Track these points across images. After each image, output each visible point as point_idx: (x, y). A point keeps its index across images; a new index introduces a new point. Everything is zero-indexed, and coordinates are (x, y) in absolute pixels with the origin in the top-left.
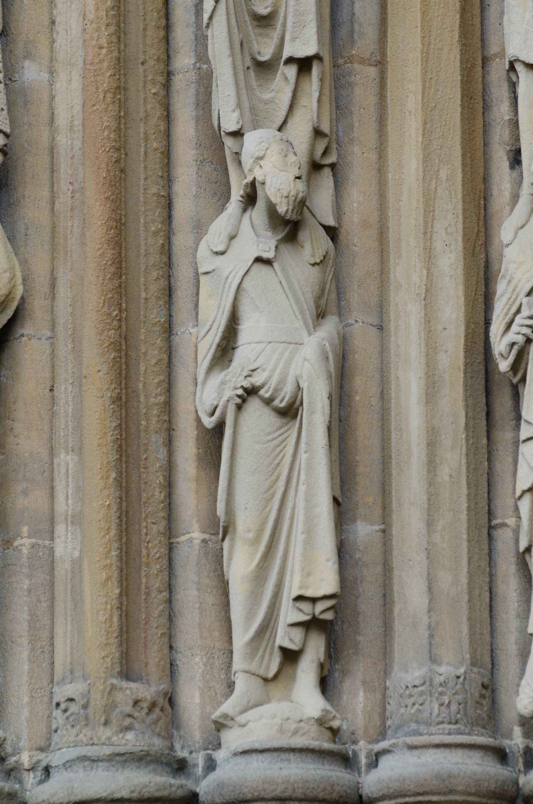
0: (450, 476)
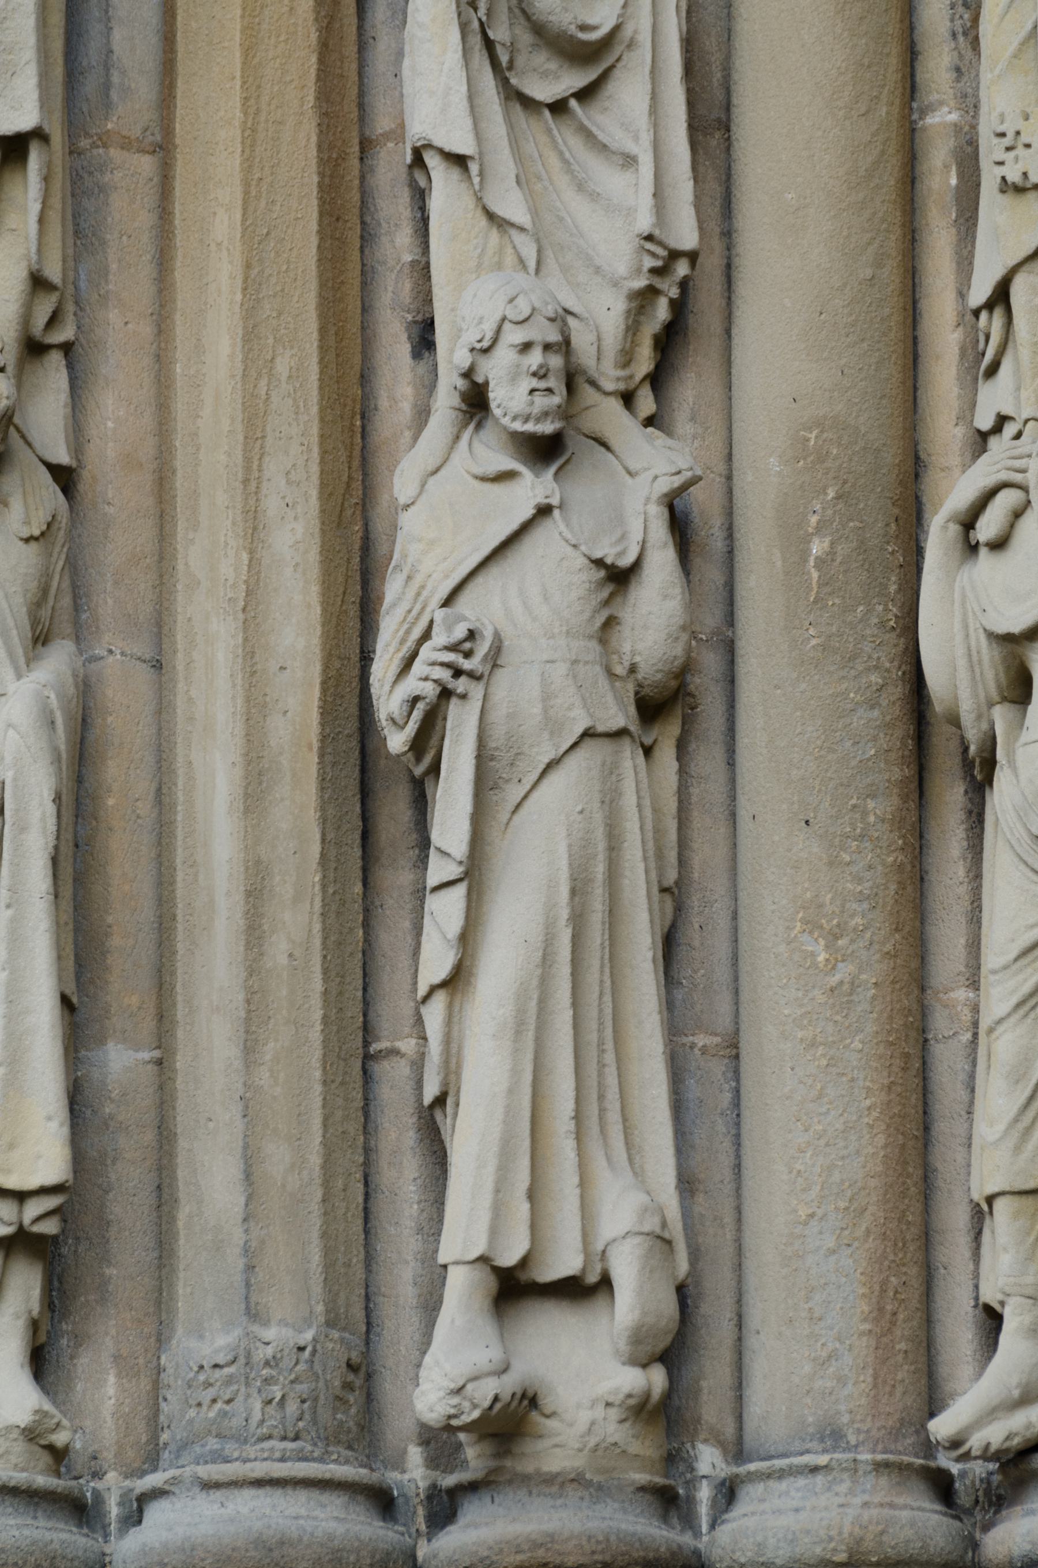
0: (290, 955)
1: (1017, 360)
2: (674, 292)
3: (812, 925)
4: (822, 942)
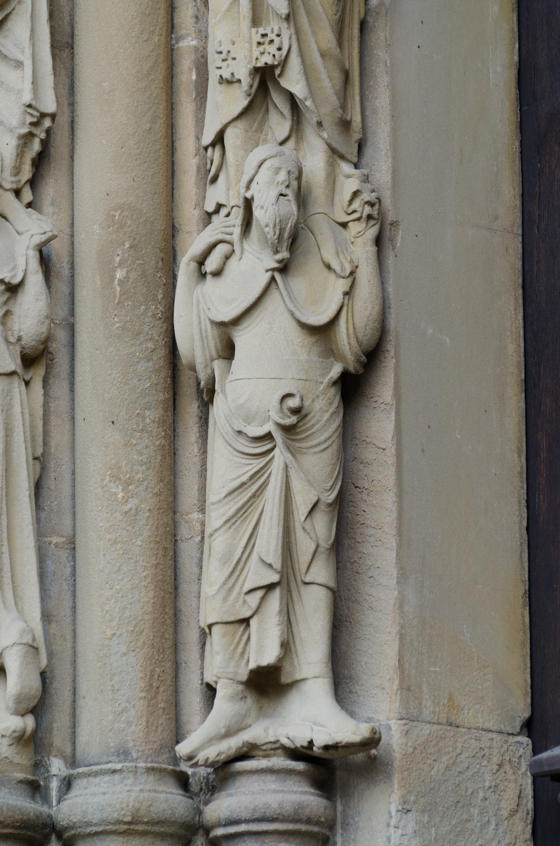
1: (227, 174)
2: (43, 136)
3: (115, 478)
4: (120, 487)
